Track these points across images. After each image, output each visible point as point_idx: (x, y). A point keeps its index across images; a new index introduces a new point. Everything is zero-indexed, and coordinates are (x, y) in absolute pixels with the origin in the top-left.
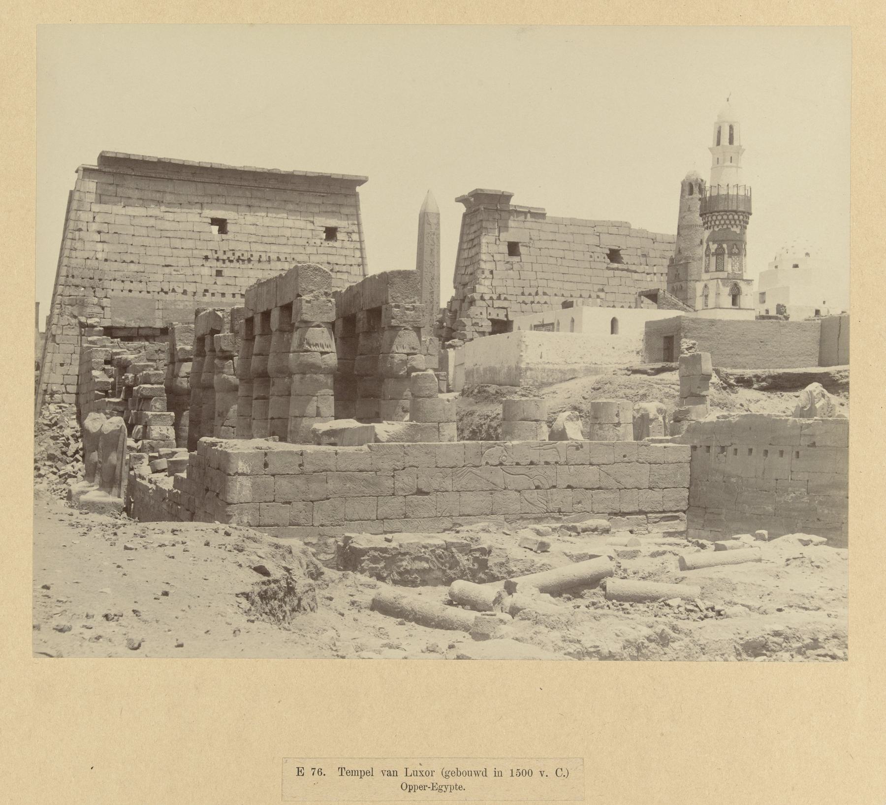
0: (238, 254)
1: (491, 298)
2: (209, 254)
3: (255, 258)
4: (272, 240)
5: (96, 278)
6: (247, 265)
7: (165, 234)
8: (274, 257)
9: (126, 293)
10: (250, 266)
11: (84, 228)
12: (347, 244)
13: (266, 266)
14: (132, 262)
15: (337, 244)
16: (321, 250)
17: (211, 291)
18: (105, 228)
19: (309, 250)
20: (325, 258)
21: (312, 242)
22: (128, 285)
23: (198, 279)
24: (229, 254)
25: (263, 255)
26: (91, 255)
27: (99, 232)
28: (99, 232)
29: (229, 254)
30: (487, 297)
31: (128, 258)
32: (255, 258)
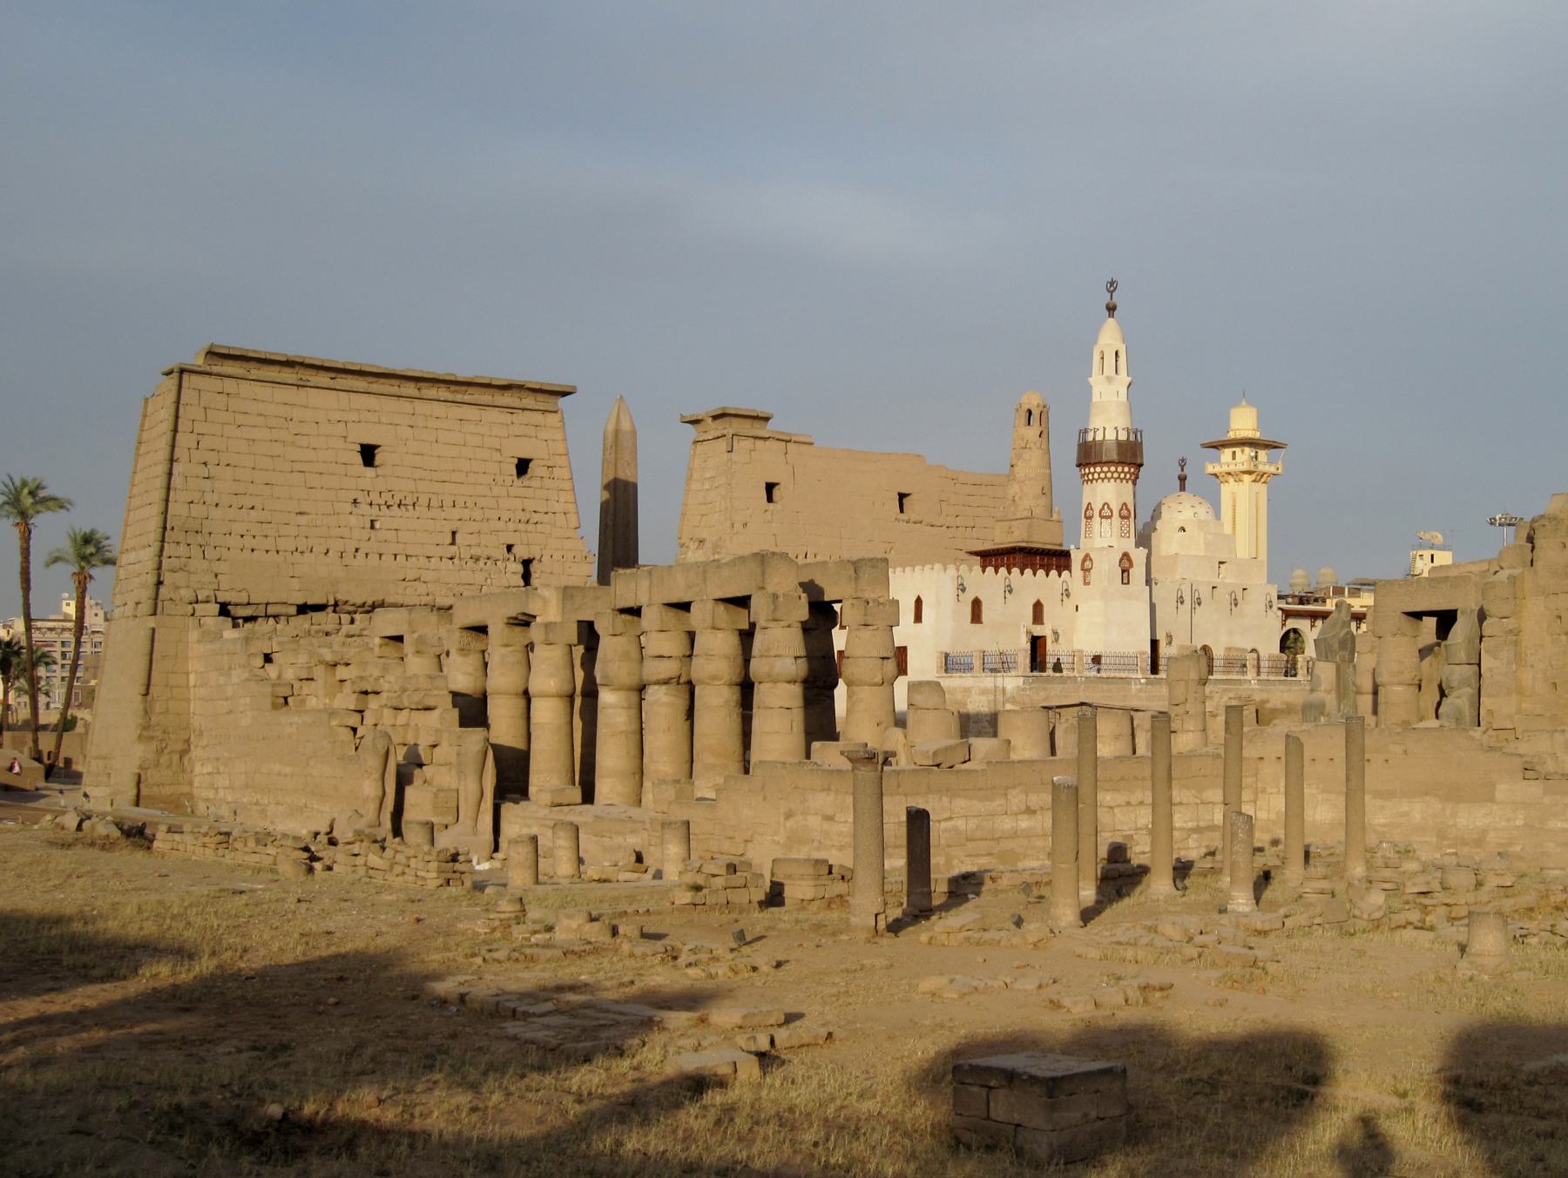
2: (361, 497)
3: (423, 501)
7: (298, 467)
8: (448, 502)
9: (247, 552)
12: (547, 482)
13: (435, 512)
18: (212, 458)
19: (496, 490)
20: (518, 504)
21: (499, 479)
22: (248, 542)
23: (345, 532)
24: (387, 496)
25: (434, 498)
26: (196, 497)
31: (248, 502)
32: (423, 501)
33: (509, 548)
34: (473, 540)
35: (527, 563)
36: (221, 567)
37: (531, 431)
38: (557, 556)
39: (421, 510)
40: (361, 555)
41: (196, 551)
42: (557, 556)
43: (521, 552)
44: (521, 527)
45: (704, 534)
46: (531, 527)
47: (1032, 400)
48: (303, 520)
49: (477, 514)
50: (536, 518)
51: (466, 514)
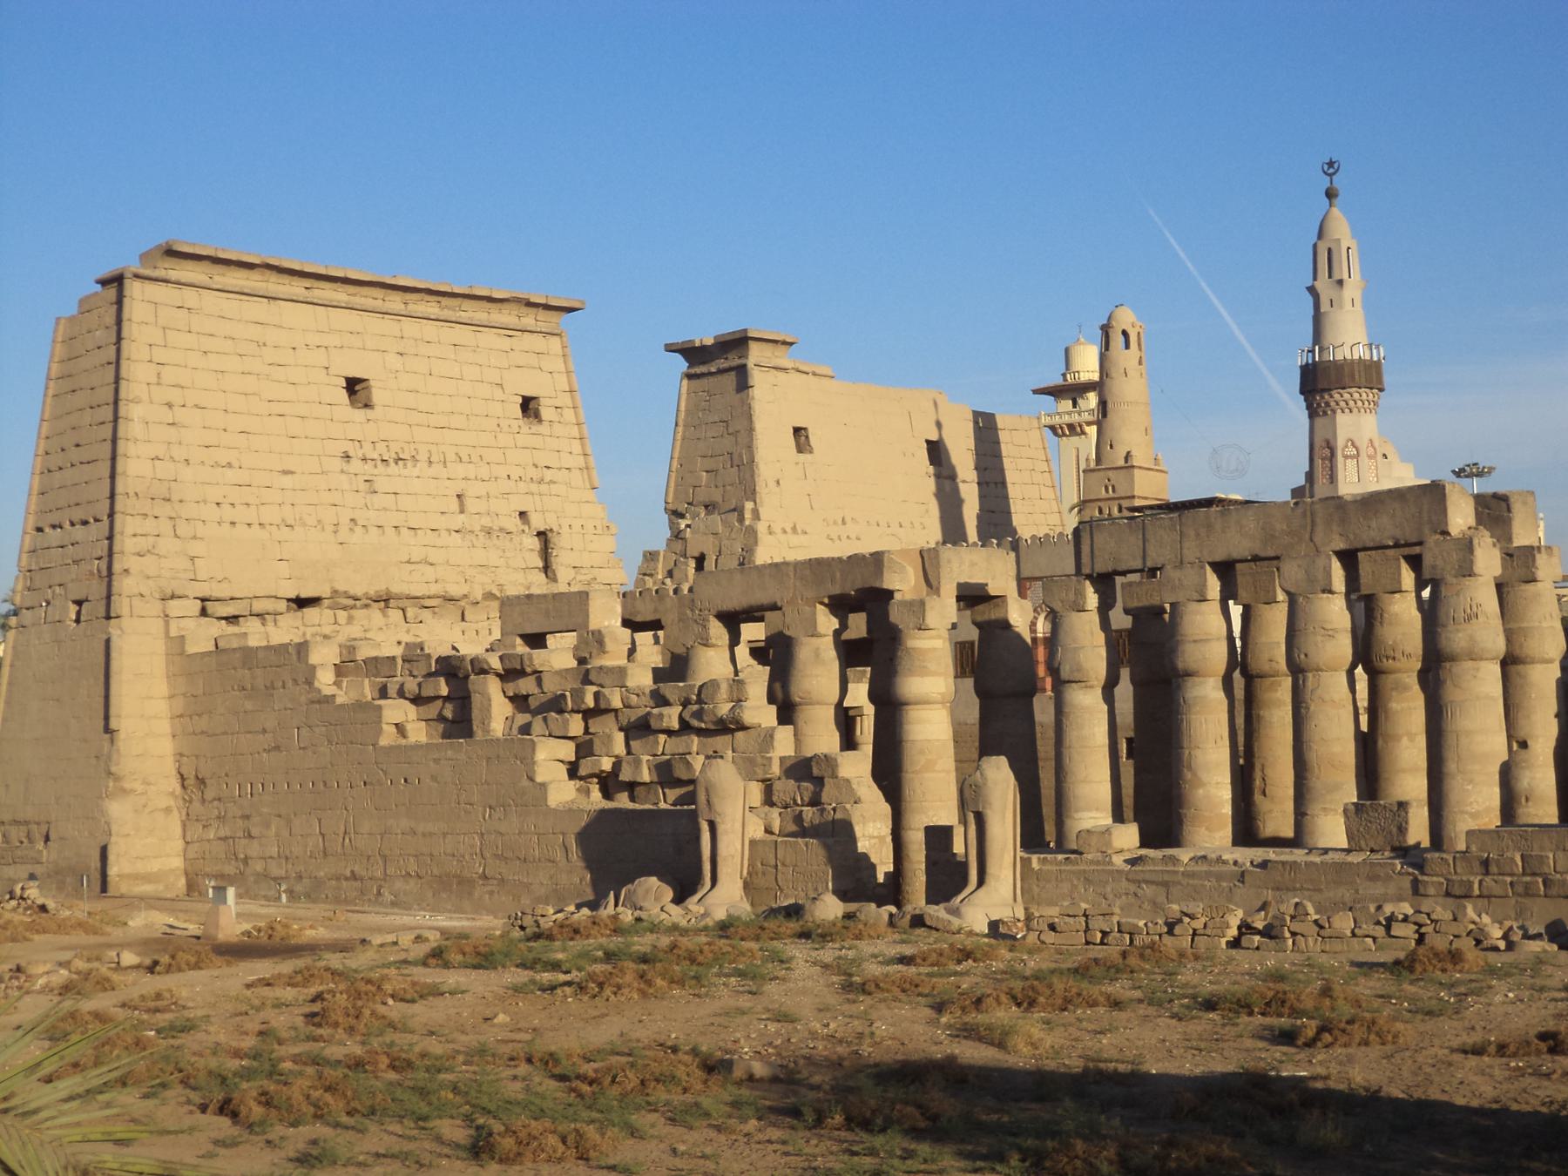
0: (395, 447)
1: (785, 532)
3: (423, 456)
4: (443, 421)
5: (175, 498)
6: (411, 470)
9: (226, 526)
10: (416, 472)
11: (145, 397)
13: (437, 469)
14: (229, 465)
15: (543, 428)
16: (522, 440)
17: (361, 522)
18: (175, 396)
21: (504, 423)
22: (228, 513)
26: (160, 450)
27: (170, 405)
28: (170, 405)
29: (381, 447)
30: (777, 529)
32: (423, 456)
33: (522, 514)
34: (481, 506)
35: (542, 535)
36: (196, 548)
37: (533, 360)
38: (577, 527)
39: (423, 465)
40: (358, 529)
41: (165, 526)
42: (577, 527)
43: (538, 523)
44: (534, 487)
45: (717, 496)
46: (544, 488)
47: (1126, 318)
48: (287, 481)
49: (484, 472)
50: (549, 475)
51: (471, 471)
